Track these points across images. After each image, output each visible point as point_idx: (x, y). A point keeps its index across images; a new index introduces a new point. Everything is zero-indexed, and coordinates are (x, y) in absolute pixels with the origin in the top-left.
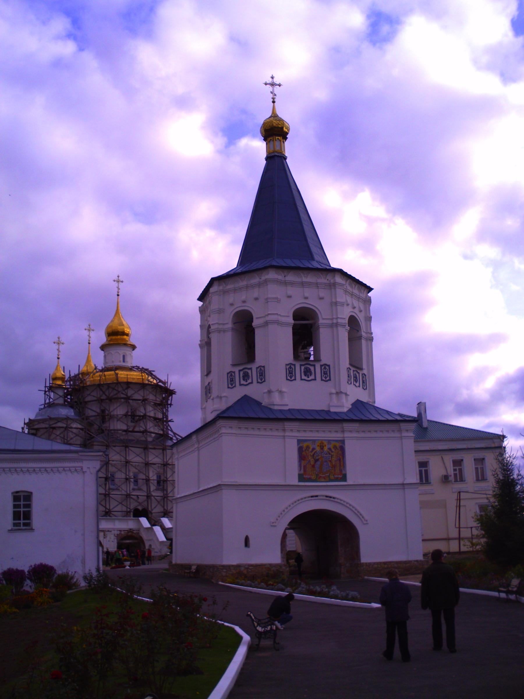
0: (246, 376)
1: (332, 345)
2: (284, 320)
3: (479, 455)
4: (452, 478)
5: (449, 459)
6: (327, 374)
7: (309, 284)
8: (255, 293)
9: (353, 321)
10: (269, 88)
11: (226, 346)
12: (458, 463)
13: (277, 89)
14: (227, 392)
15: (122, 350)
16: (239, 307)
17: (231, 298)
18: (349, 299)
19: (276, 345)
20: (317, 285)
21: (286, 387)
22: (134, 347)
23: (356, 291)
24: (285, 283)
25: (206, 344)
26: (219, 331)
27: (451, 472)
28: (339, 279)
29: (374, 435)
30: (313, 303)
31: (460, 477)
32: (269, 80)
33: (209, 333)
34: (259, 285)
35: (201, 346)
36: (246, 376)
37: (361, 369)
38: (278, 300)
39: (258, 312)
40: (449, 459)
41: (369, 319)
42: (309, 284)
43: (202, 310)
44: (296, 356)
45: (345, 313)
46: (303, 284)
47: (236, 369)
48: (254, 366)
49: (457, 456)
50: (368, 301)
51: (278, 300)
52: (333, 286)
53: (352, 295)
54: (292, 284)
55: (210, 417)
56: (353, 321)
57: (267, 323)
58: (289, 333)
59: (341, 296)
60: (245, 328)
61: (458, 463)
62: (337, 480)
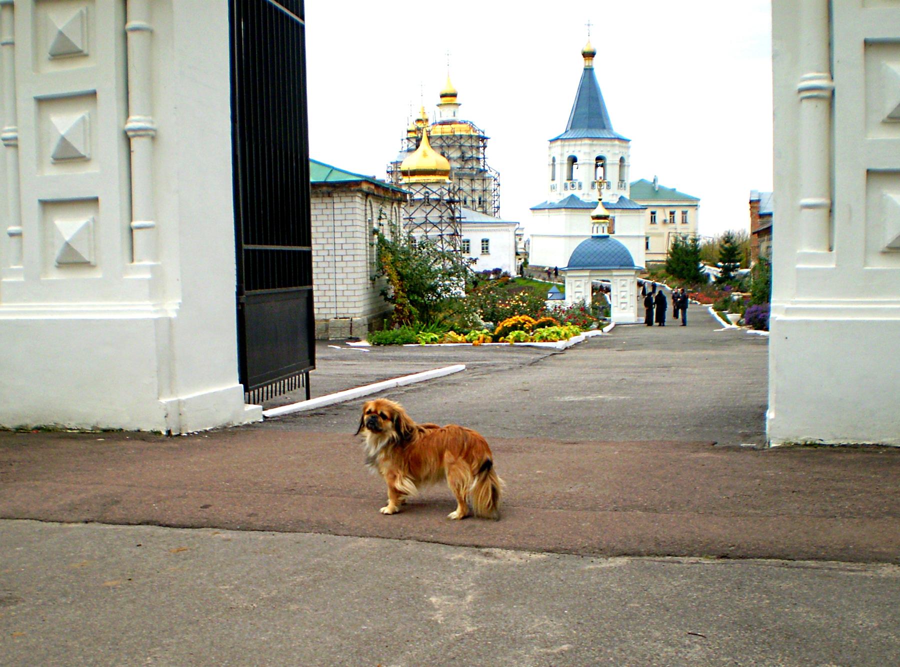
0: (573, 186)
1: (612, 173)
3: (685, 209)
4: (668, 221)
5: (668, 211)
8: (578, 148)
11: (562, 171)
12: (672, 213)
14: (564, 192)
15: (452, 109)
16: (571, 154)
17: (566, 149)
27: (668, 218)
28: (617, 142)
31: (672, 221)
36: (573, 186)
40: (668, 211)
47: (569, 182)
49: (672, 210)
61: (672, 213)
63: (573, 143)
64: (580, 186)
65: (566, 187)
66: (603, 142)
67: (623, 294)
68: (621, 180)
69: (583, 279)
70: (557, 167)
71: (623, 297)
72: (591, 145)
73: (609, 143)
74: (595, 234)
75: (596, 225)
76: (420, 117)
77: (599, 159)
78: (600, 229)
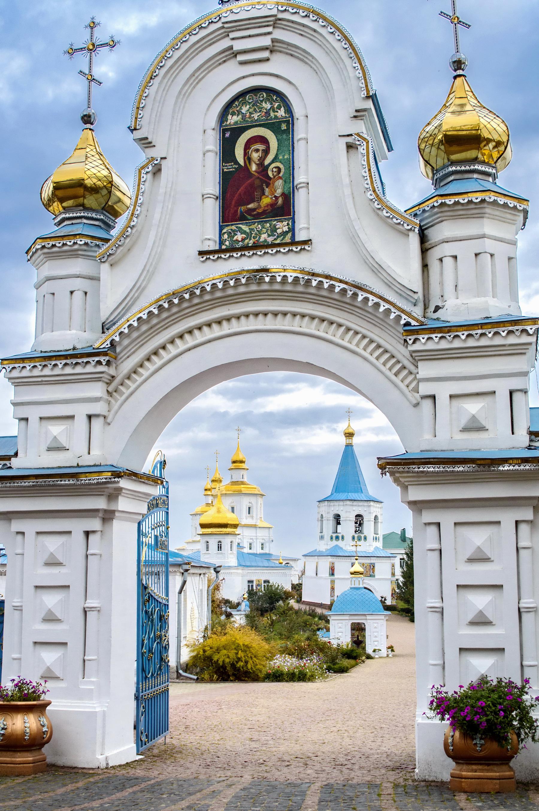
1: (368, 528)
2: (351, 519)
6: (365, 538)
7: (361, 505)
11: (329, 525)
14: (330, 543)
15: (242, 472)
19: (347, 528)
24: (353, 505)
28: (372, 503)
29: (381, 561)
38: (350, 512)
47: (334, 535)
51: (350, 512)
60: (337, 519)
62: (368, 576)
64: (343, 538)
66: (361, 503)
67: (376, 634)
69: (344, 622)
71: (376, 637)
73: (366, 504)
74: (353, 586)
75: (354, 579)
77: (356, 516)
78: (357, 582)
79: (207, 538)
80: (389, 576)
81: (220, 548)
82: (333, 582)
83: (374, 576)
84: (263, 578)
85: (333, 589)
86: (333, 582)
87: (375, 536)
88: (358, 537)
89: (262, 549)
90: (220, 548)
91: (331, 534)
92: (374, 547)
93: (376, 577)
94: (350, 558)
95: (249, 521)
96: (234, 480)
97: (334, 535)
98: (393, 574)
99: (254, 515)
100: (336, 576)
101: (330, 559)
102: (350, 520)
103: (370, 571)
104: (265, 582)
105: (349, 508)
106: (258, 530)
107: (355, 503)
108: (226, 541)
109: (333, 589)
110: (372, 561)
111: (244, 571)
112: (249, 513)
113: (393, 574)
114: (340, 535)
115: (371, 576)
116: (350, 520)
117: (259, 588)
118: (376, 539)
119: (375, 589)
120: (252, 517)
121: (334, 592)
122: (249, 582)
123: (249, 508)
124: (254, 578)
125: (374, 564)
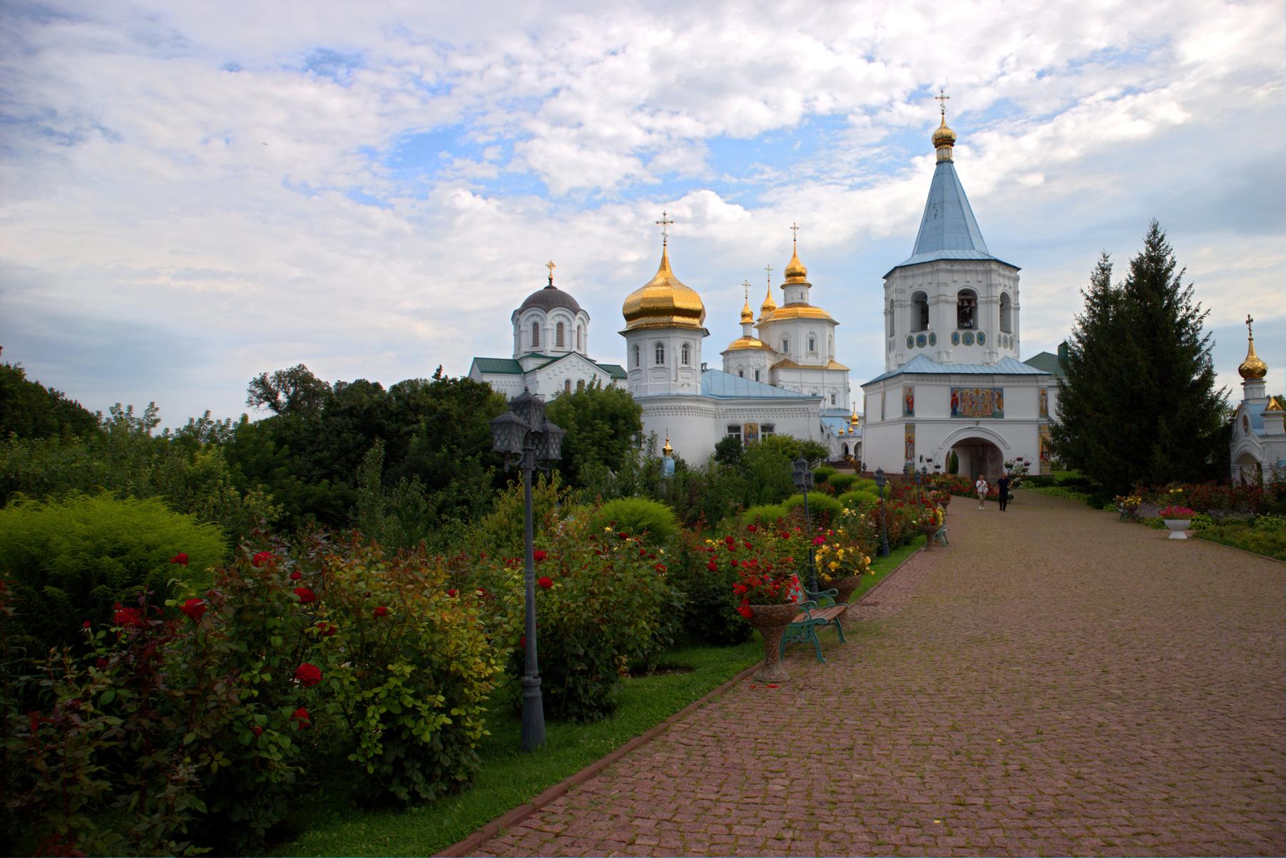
1: (987, 317)
6: (981, 339)
8: (929, 279)
9: (1004, 298)
10: (939, 101)
11: (906, 317)
13: (946, 101)
15: (800, 289)
16: (916, 289)
17: (910, 282)
18: (1001, 280)
20: (977, 272)
21: (951, 348)
22: (810, 286)
23: (1007, 273)
24: (952, 271)
25: (890, 312)
26: (901, 306)
28: (994, 266)
30: (973, 286)
32: (939, 95)
33: (892, 307)
34: (932, 273)
35: (885, 314)
37: (1009, 332)
38: (946, 284)
39: (931, 293)
41: (1018, 293)
42: (971, 271)
43: (886, 286)
44: (960, 327)
45: (998, 292)
46: (966, 272)
48: (927, 334)
50: (1017, 279)
51: (946, 284)
52: (989, 272)
53: (1004, 276)
54: (958, 271)
55: (895, 369)
56: (1004, 298)
57: (938, 302)
58: (955, 308)
59: (995, 279)
60: (922, 306)
63: (917, 271)
64: (933, 340)
65: (910, 343)
66: (971, 267)
68: (1005, 327)
70: (897, 311)
72: (947, 271)
73: (981, 268)
76: (766, 305)
79: (636, 339)
80: (1034, 416)
81: (660, 357)
82: (910, 429)
83: (1002, 415)
84: (760, 420)
85: (910, 442)
86: (910, 429)
87: (1003, 334)
88: (964, 336)
89: (833, 402)
90: (660, 357)
91: (908, 333)
92: (1001, 356)
93: (1007, 417)
94: (946, 378)
95: (811, 361)
96: (790, 301)
97: (915, 336)
98: (1044, 412)
99: (820, 351)
100: (918, 415)
101: (908, 382)
102: (947, 302)
103: (991, 404)
104: (765, 428)
105: (944, 277)
106: (826, 374)
107: (957, 267)
108: (674, 345)
109: (910, 442)
110: (997, 385)
111: (720, 407)
112: (812, 348)
113: (1044, 412)
114: (927, 334)
115: (994, 415)
116: (947, 302)
117: (751, 440)
118: (1006, 341)
119: (1003, 443)
120: (816, 354)
121: (913, 449)
122: (731, 428)
123: (812, 342)
124: (741, 420)
125: (1001, 389)
